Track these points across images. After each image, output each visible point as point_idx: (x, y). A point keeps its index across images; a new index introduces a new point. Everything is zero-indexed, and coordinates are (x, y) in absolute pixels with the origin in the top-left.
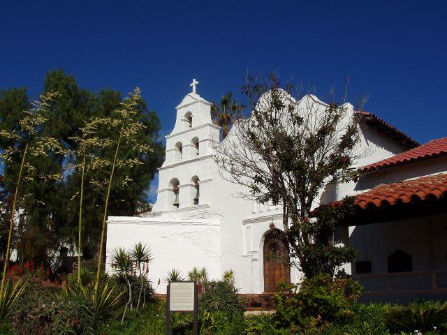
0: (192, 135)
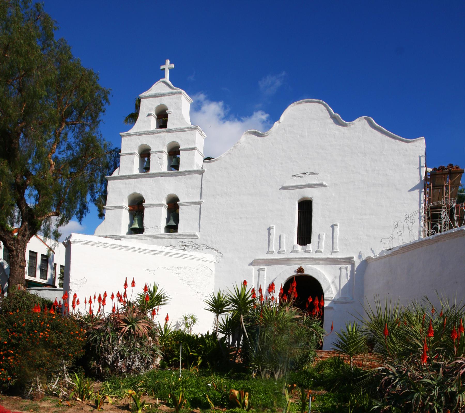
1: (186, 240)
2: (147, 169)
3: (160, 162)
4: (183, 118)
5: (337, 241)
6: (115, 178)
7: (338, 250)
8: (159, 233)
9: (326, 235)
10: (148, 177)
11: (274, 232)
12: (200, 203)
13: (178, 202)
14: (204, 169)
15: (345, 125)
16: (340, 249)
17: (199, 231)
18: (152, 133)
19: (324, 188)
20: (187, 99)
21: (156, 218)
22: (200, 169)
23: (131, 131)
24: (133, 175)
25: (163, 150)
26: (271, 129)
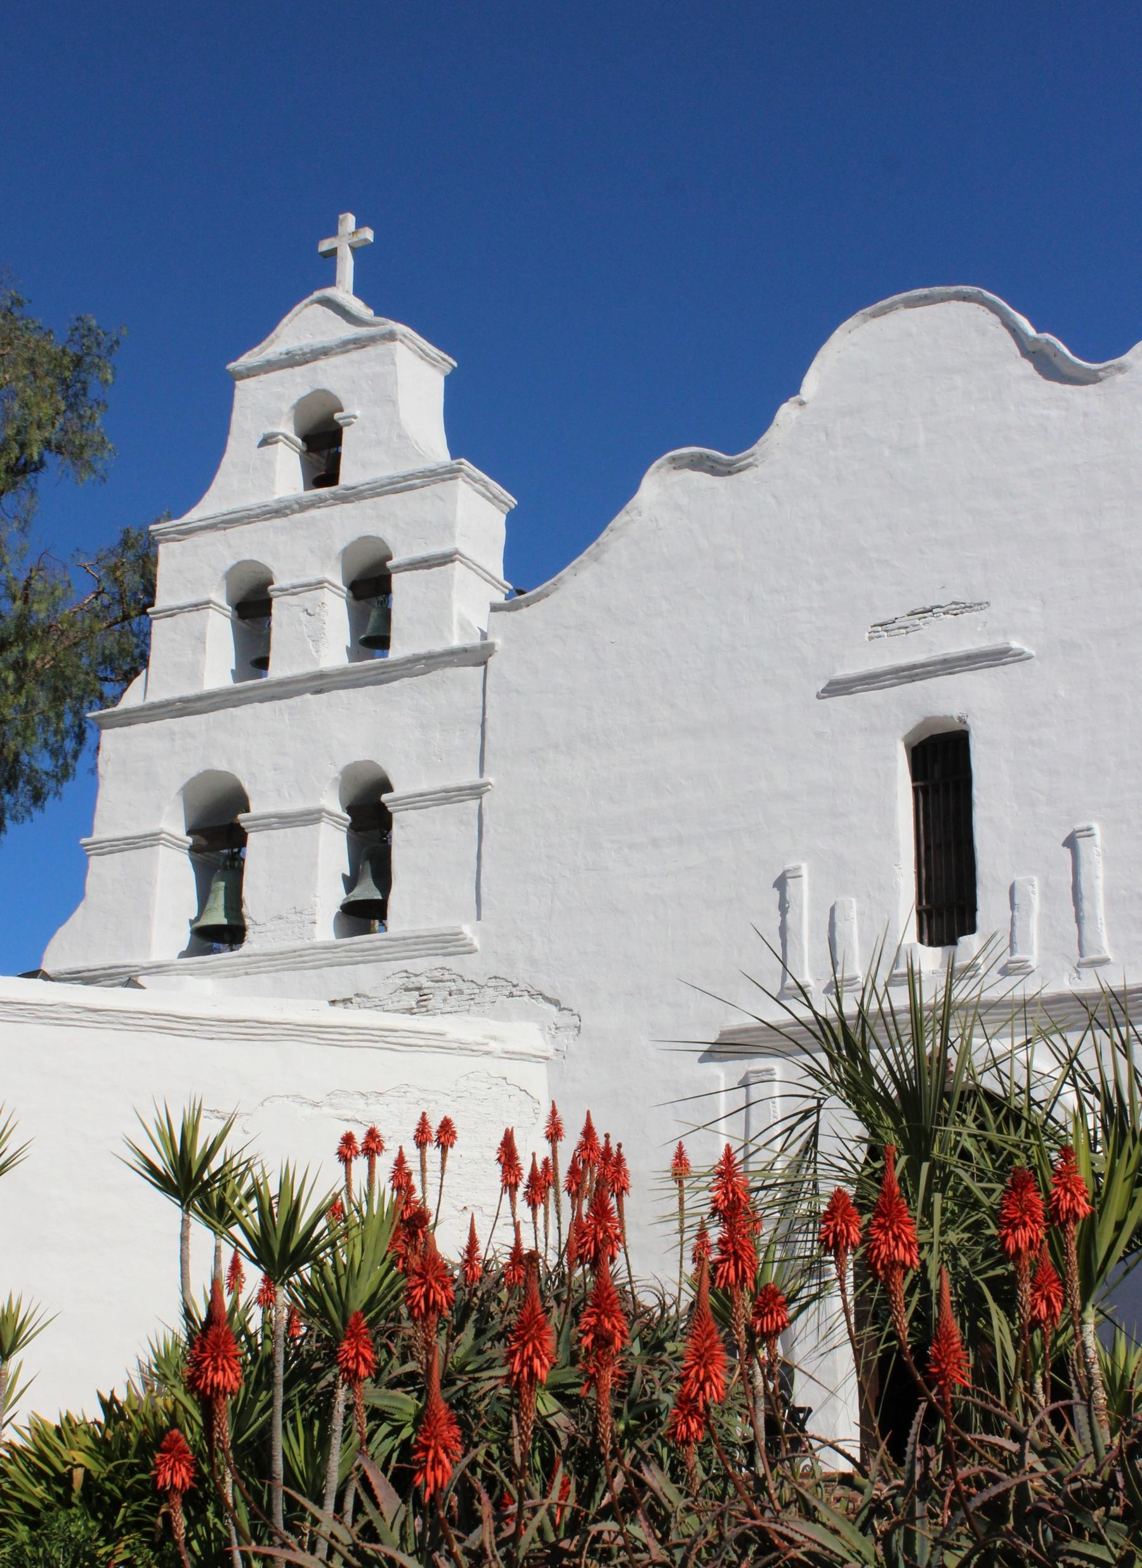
0: (342, 525)
1: (420, 965)
2: (262, 664)
3: (315, 630)
4: (403, 437)
5: (1098, 908)
6: (131, 718)
7: (1108, 953)
8: (307, 943)
9: (1046, 885)
10: (261, 701)
11: (803, 892)
12: (477, 791)
13: (385, 797)
14: (490, 640)
15: (1090, 379)
16: (1115, 946)
17: (479, 918)
18: (279, 511)
19: (1014, 670)
20: (424, 356)
21: (298, 873)
22: (476, 641)
23: (194, 516)
24: (199, 698)
25: (319, 576)
26: (767, 435)
